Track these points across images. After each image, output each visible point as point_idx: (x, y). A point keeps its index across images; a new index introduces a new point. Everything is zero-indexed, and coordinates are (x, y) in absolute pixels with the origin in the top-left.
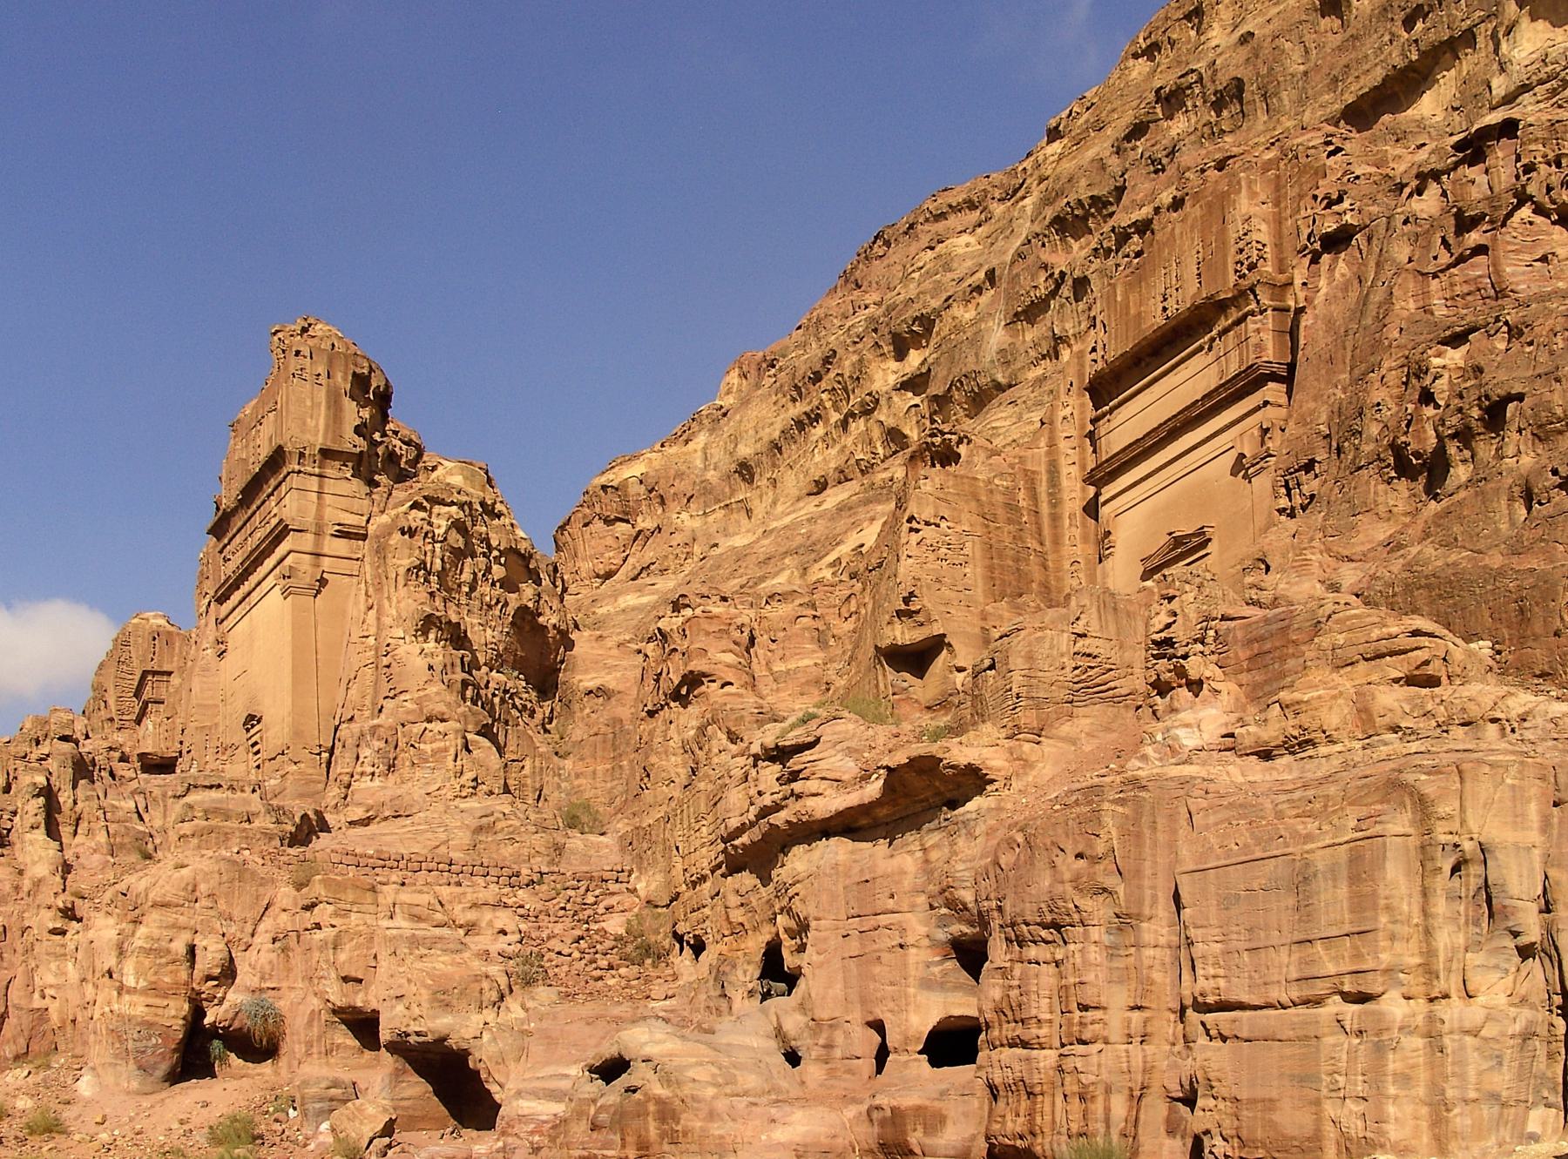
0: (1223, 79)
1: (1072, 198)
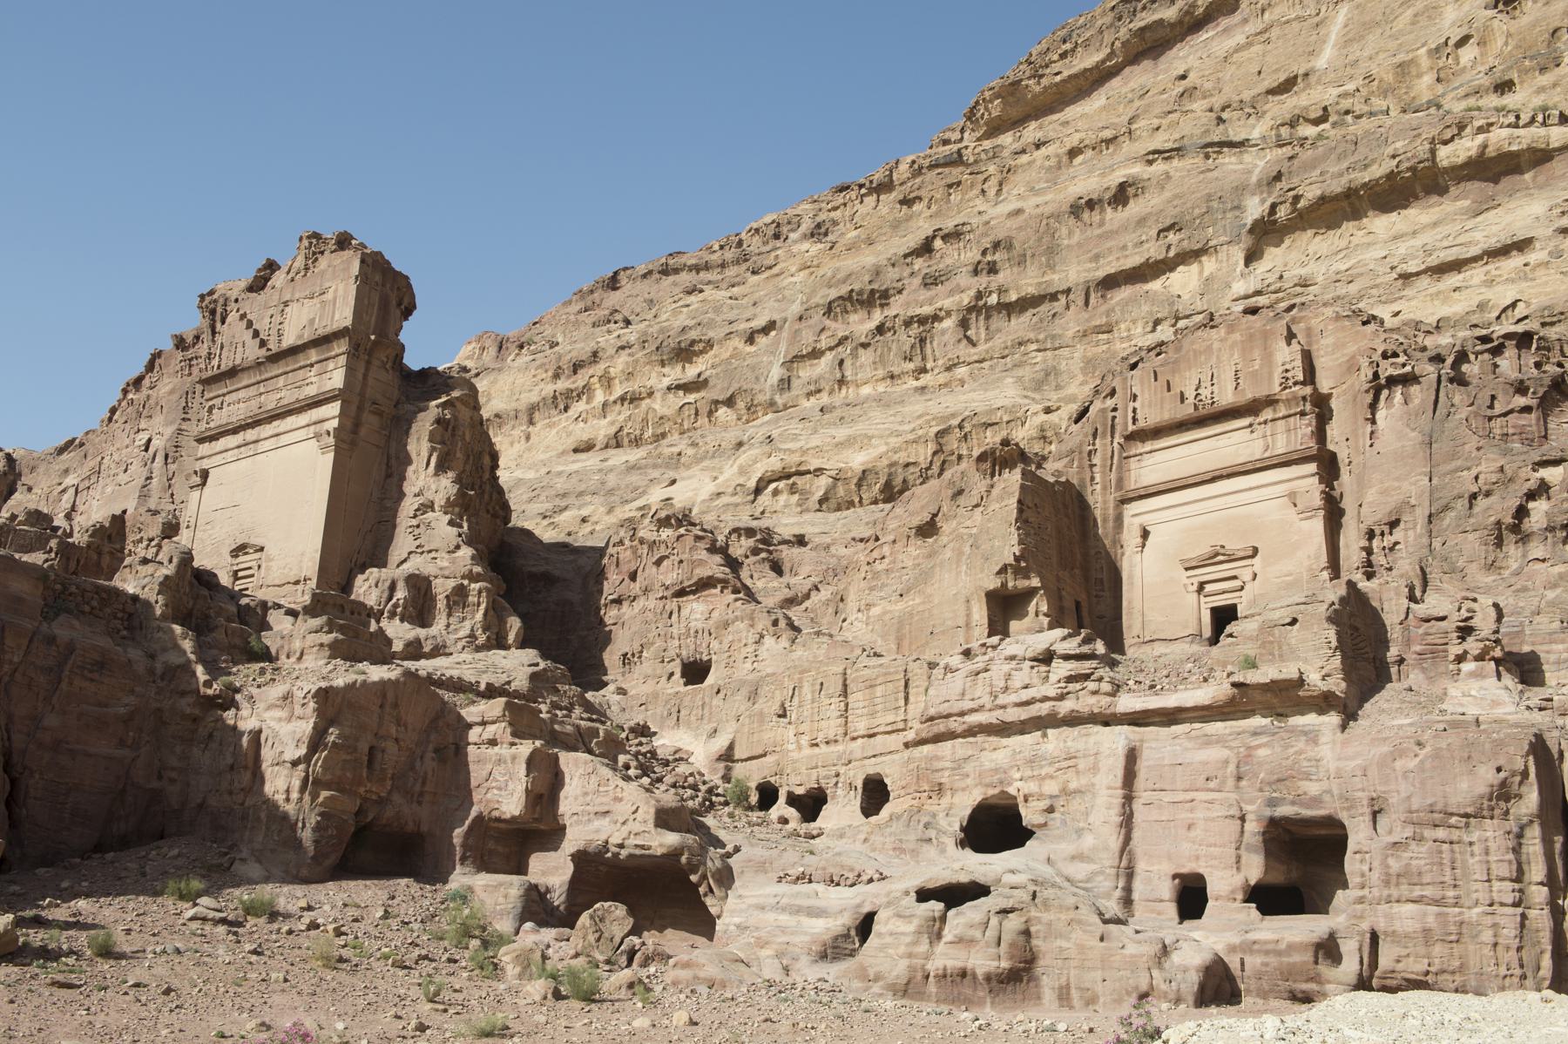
1: (857, 287)
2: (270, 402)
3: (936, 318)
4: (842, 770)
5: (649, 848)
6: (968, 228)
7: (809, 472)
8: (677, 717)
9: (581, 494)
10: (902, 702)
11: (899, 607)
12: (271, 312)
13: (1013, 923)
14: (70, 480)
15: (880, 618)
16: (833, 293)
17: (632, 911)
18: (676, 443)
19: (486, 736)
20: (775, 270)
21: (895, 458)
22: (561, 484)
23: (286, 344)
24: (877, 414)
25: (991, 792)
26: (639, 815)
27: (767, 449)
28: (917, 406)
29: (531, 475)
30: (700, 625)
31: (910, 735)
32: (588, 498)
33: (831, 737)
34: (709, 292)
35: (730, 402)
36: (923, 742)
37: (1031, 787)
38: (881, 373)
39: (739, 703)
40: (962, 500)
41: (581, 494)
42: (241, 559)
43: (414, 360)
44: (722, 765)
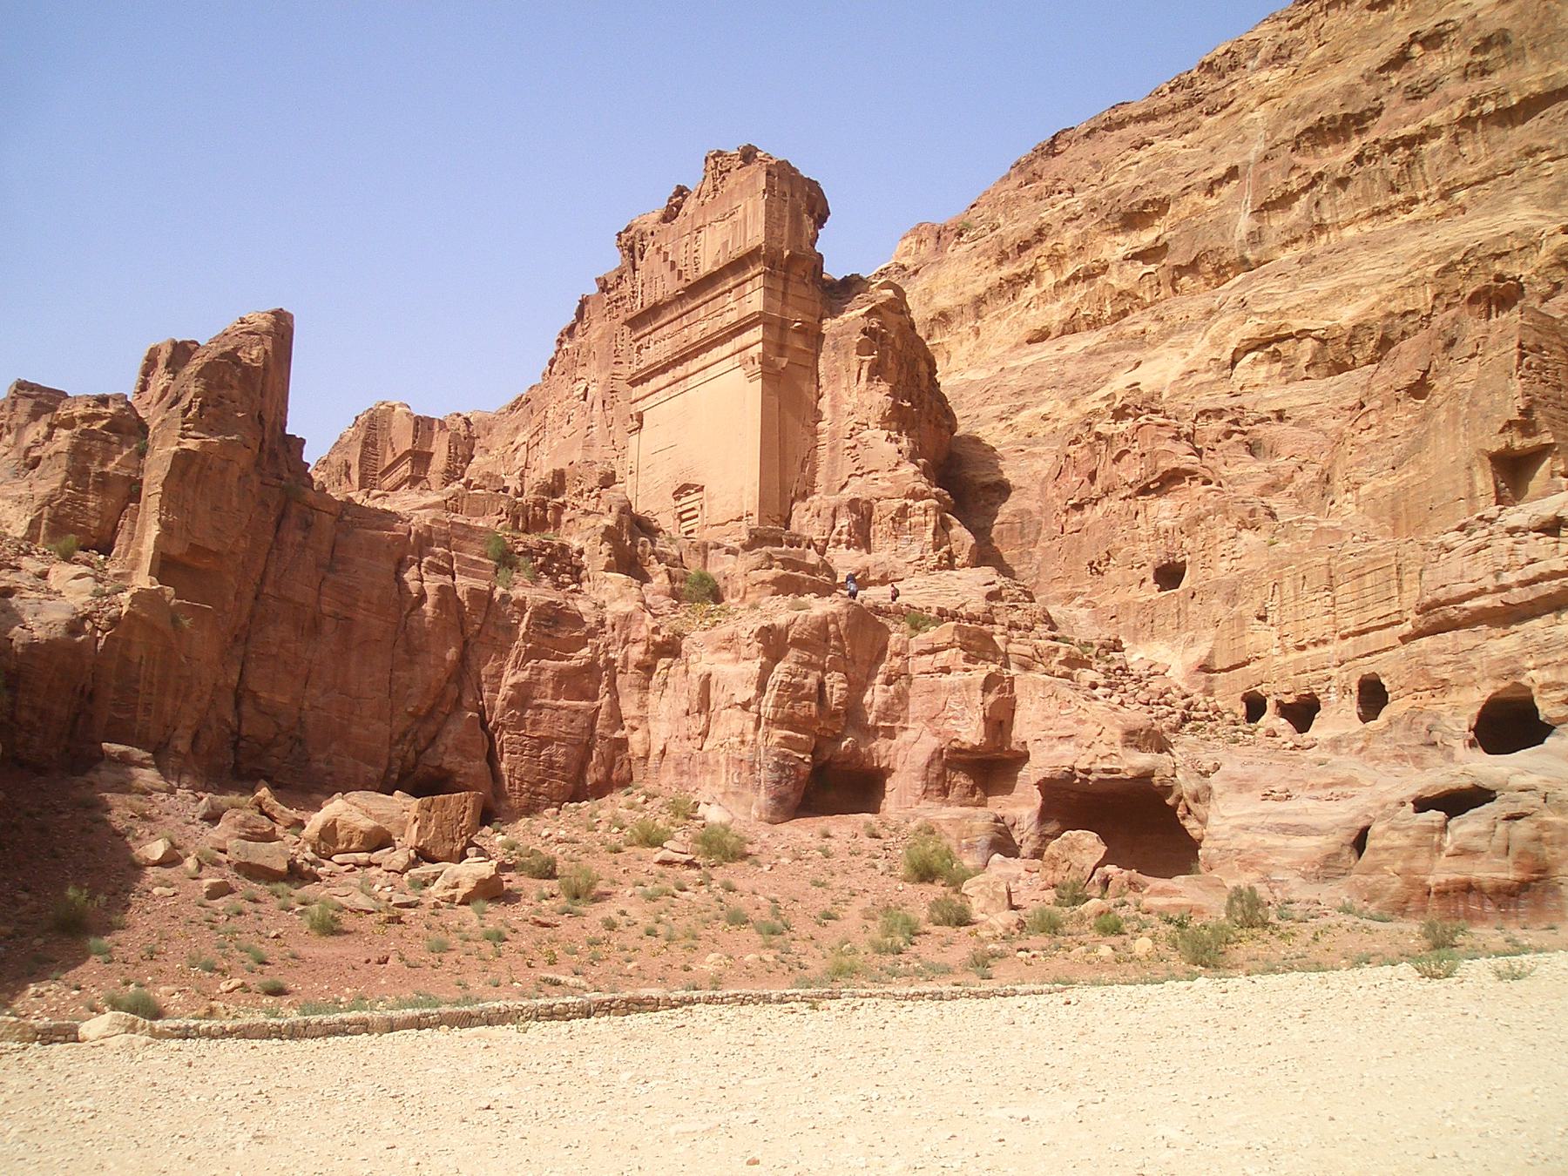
0: (1489, 29)
1: (1326, 114)
2: (695, 334)
3: (1421, 138)
4: (1334, 672)
5: (1119, 771)
6: (1451, 26)
7: (1290, 336)
8: (1148, 626)
9: (1040, 388)
10: (1395, 592)
11: (1392, 481)
12: (686, 239)
13: (1523, 829)
14: (522, 438)
15: (1370, 497)
16: (1300, 125)
17: (1105, 838)
18: (1139, 321)
19: (938, 664)
20: (1232, 108)
21: (1392, 306)
22: (1015, 381)
23: (702, 273)
24: (1363, 258)
25: (1502, 685)
26: (1106, 736)
27: (1241, 314)
28: (1410, 244)
29: (982, 375)
30: (1168, 523)
31: (1407, 628)
32: (1046, 393)
33: (1319, 636)
34: (1160, 144)
35: (1192, 268)
36: (1419, 634)
37: (1548, 675)
38: (1364, 210)
39: (1218, 608)
40: (1454, 352)
41: (1040, 388)
42: (684, 500)
43: (835, 270)
44: (1204, 675)
